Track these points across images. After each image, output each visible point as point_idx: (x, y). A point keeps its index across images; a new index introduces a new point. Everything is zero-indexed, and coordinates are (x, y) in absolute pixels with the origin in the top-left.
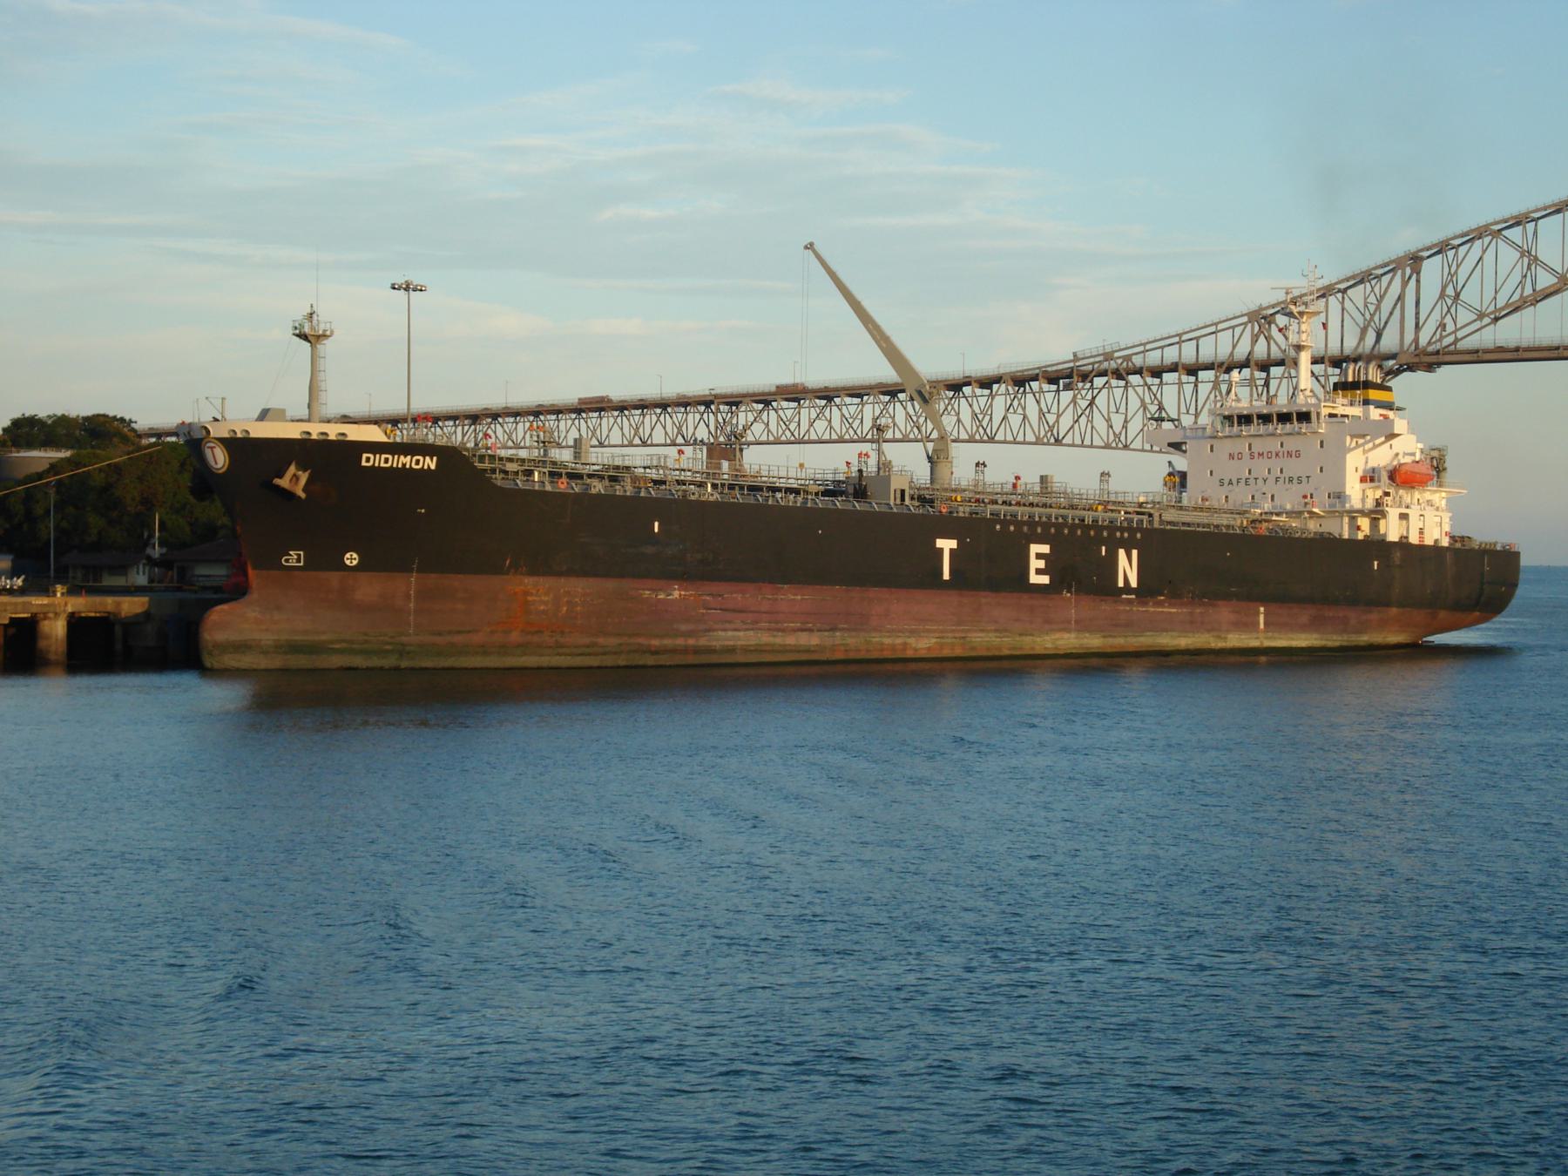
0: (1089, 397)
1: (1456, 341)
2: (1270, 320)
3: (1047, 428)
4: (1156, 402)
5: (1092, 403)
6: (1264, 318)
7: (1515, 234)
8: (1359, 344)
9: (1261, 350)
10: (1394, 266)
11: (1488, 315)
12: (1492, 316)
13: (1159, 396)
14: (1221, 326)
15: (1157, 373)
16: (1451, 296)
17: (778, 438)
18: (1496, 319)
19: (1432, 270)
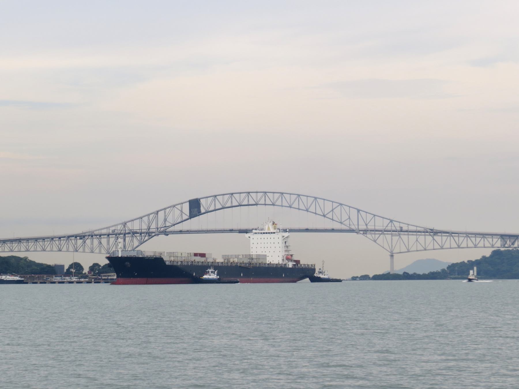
7: (179, 207)
15: (100, 236)
16: (165, 220)
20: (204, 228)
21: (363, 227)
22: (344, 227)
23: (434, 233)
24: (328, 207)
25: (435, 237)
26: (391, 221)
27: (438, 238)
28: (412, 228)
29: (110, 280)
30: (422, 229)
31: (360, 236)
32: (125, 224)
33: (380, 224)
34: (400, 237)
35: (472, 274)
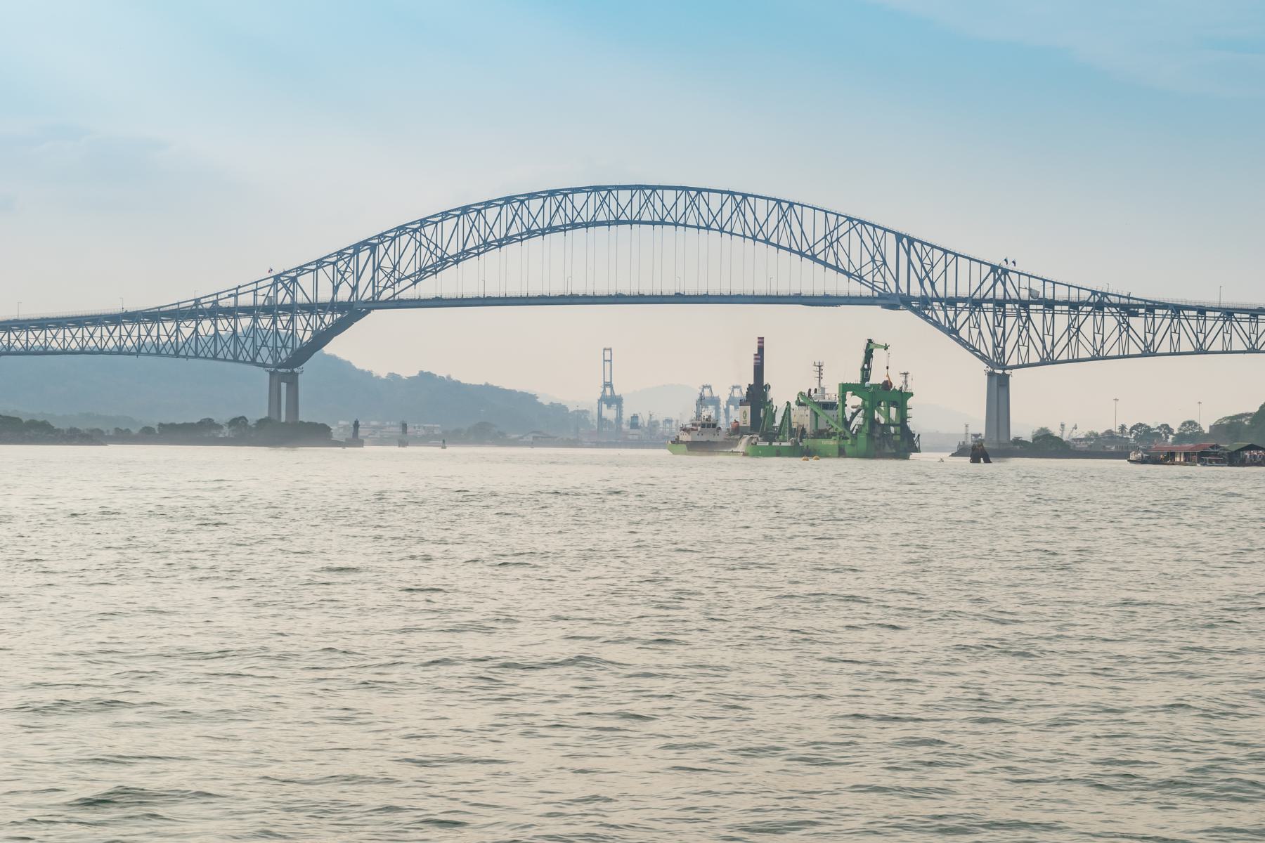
0: (194, 324)
1: (394, 295)
2: (294, 280)
3: (203, 345)
4: (230, 329)
5: (196, 329)
6: (290, 278)
8: (352, 295)
9: (288, 300)
10: (357, 248)
11: (408, 277)
12: (413, 279)
13: (232, 324)
14: (260, 285)
17: (102, 350)
18: (415, 283)
19: (381, 249)
20: (493, 291)
21: (916, 291)
22: (866, 291)
23: (1128, 309)
24: (814, 228)
25: (1132, 320)
26: (999, 272)
27: (1190, 324)
28: (1062, 293)
29: (100, 432)
30: (1085, 295)
31: (905, 315)
32: (287, 279)
33: (966, 281)
34: (1029, 318)
35: (680, 439)
